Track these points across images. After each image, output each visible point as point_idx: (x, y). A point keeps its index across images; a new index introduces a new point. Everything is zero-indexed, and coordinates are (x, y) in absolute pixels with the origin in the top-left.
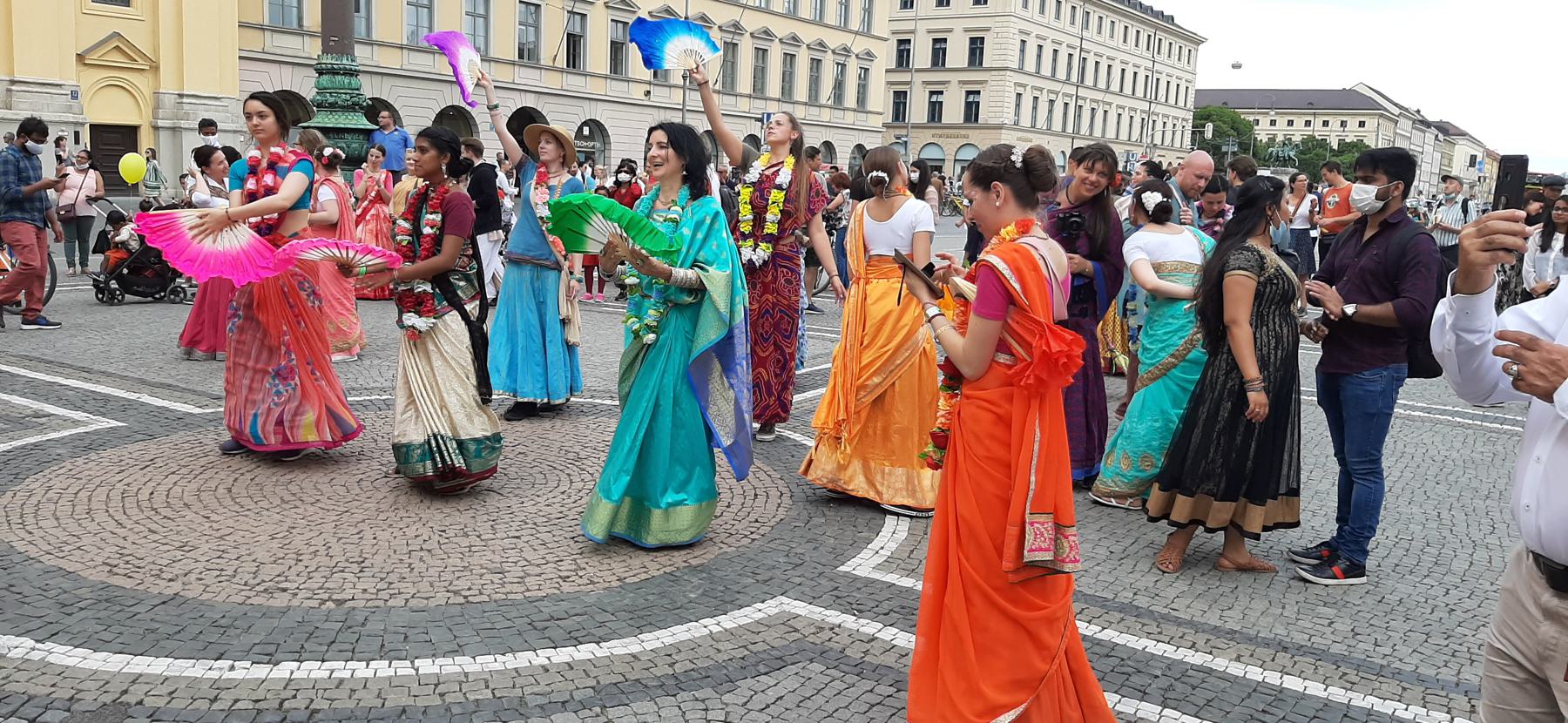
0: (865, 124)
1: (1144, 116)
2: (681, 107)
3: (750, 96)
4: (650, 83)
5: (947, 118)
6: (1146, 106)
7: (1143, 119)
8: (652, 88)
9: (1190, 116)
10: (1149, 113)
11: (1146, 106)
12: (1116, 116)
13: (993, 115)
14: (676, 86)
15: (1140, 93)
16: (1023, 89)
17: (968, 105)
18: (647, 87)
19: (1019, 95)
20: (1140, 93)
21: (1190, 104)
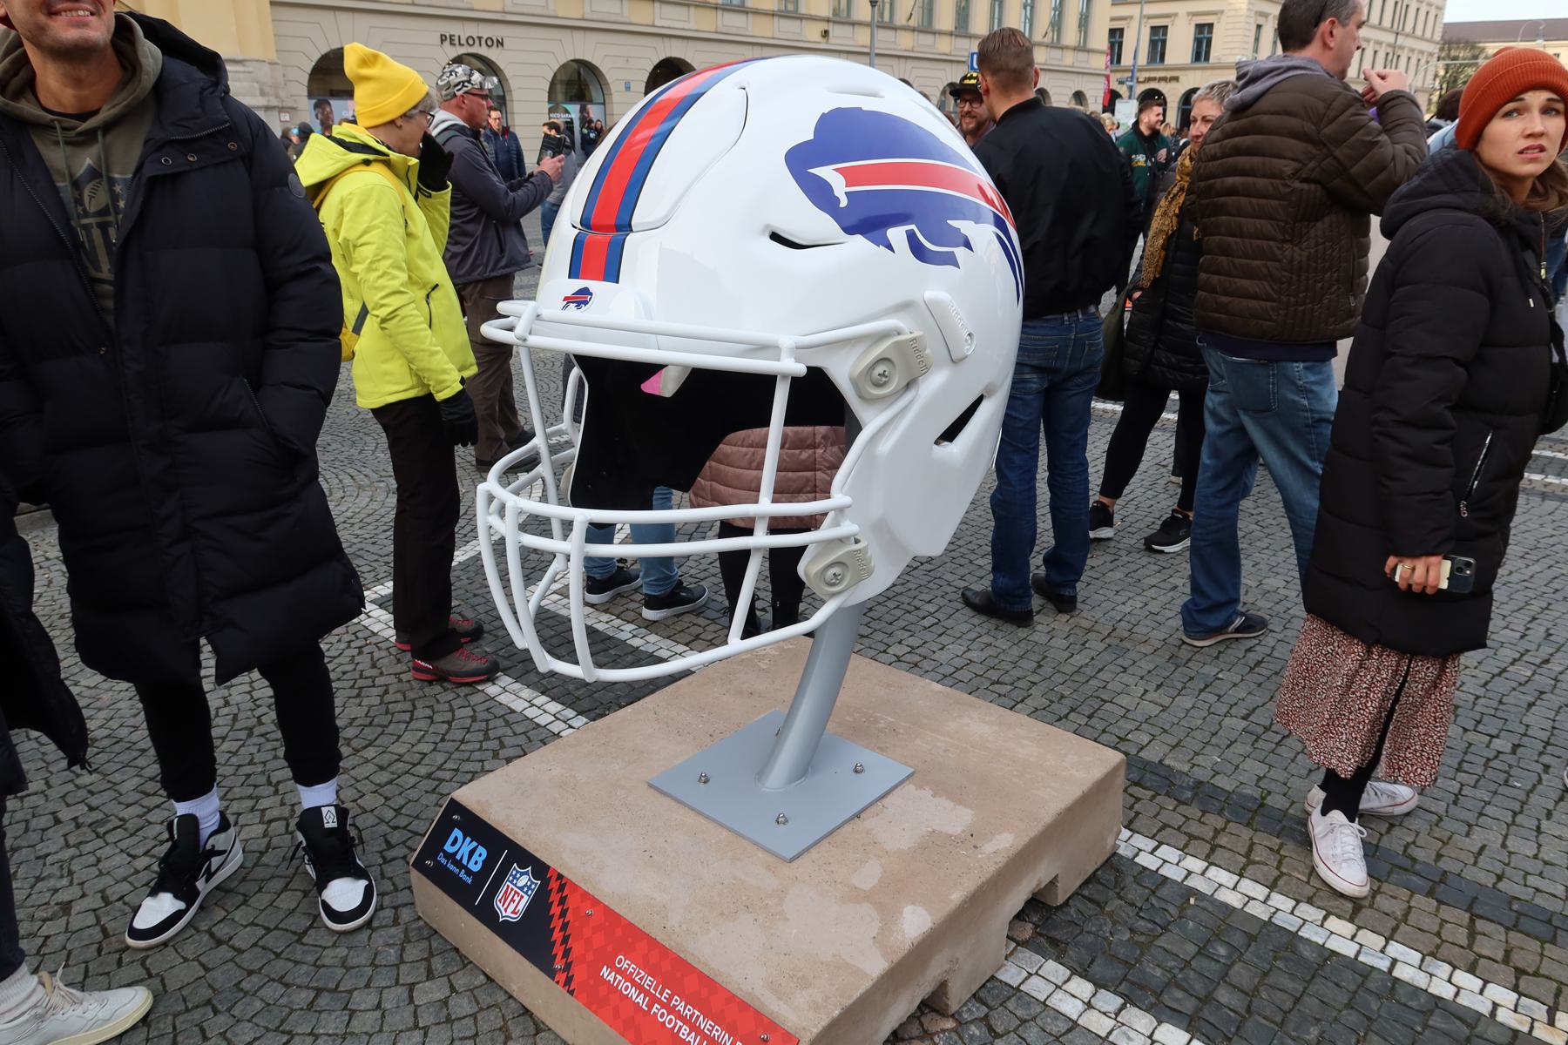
0: (1060, 63)
1: (1390, 50)
2: (868, 50)
3: (951, 34)
4: (828, 21)
5: (1170, 59)
6: (1390, 38)
7: (1387, 54)
8: (830, 27)
9: (1434, 48)
10: (1393, 46)
11: (1390, 38)
12: (1372, 53)
13: (1227, 52)
14: (861, 24)
15: (1387, 23)
16: (1264, 19)
17: (1198, 42)
18: (824, 26)
19: (1259, 27)
20: (1387, 23)
21: (1437, 37)
